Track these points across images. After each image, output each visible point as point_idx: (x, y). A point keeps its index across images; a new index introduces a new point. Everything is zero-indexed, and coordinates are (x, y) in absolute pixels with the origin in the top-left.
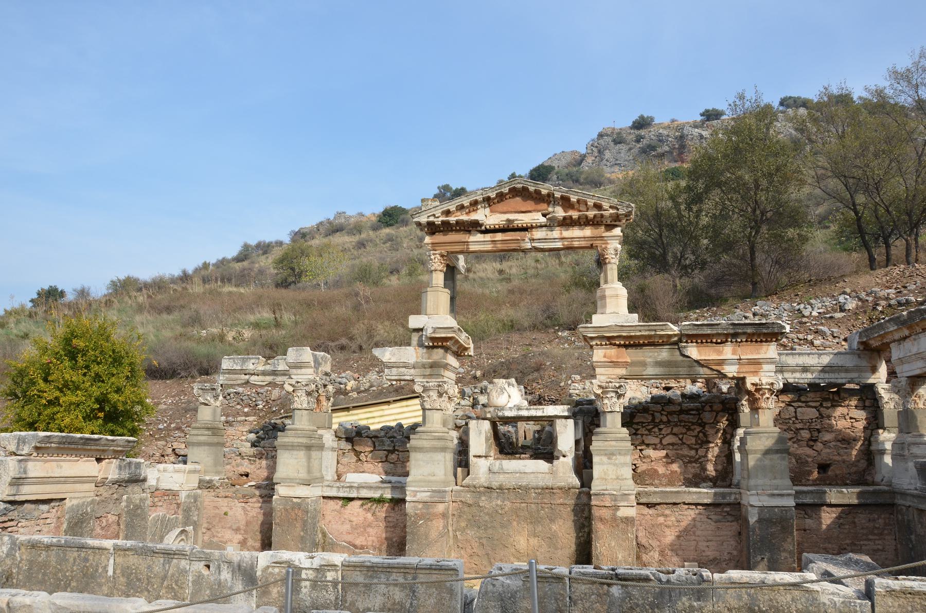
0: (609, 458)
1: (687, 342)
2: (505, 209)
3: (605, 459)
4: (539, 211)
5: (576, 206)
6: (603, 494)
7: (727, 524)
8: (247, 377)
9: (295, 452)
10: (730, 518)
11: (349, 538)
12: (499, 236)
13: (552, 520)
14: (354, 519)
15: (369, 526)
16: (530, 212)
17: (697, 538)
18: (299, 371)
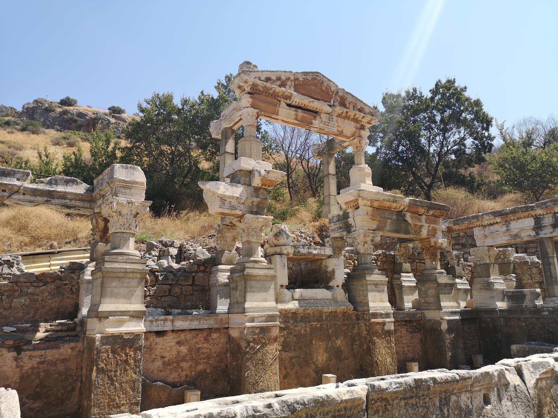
0: (376, 287)
1: (406, 211)
2: (304, 92)
3: (373, 287)
4: (325, 101)
5: (348, 105)
6: (377, 313)
7: (416, 334)
8: (6, 194)
9: (127, 281)
10: (417, 330)
11: (162, 375)
12: (300, 113)
13: (337, 338)
14: (167, 354)
15: (183, 359)
16: (319, 100)
17: (403, 345)
18: (128, 191)
